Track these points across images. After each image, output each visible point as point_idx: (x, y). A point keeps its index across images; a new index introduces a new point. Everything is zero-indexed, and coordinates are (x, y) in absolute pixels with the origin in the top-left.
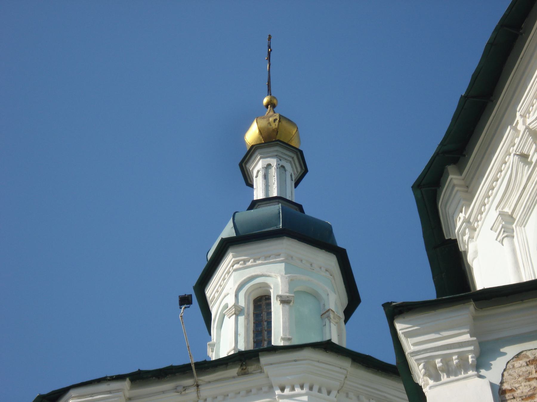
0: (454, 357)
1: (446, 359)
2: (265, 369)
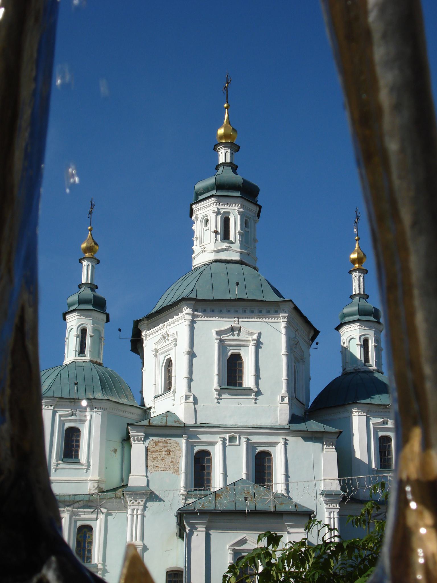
0: (139, 438)
1: (138, 438)
2: (92, 403)
